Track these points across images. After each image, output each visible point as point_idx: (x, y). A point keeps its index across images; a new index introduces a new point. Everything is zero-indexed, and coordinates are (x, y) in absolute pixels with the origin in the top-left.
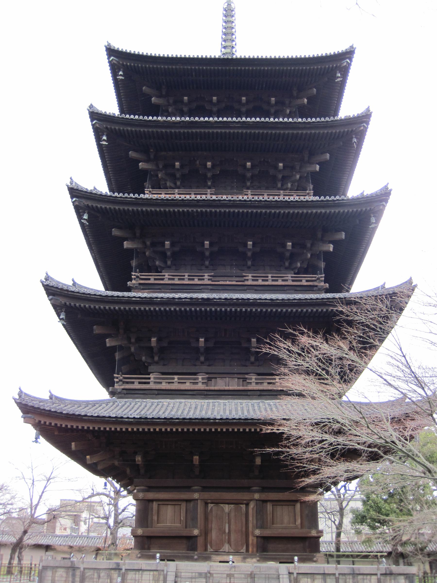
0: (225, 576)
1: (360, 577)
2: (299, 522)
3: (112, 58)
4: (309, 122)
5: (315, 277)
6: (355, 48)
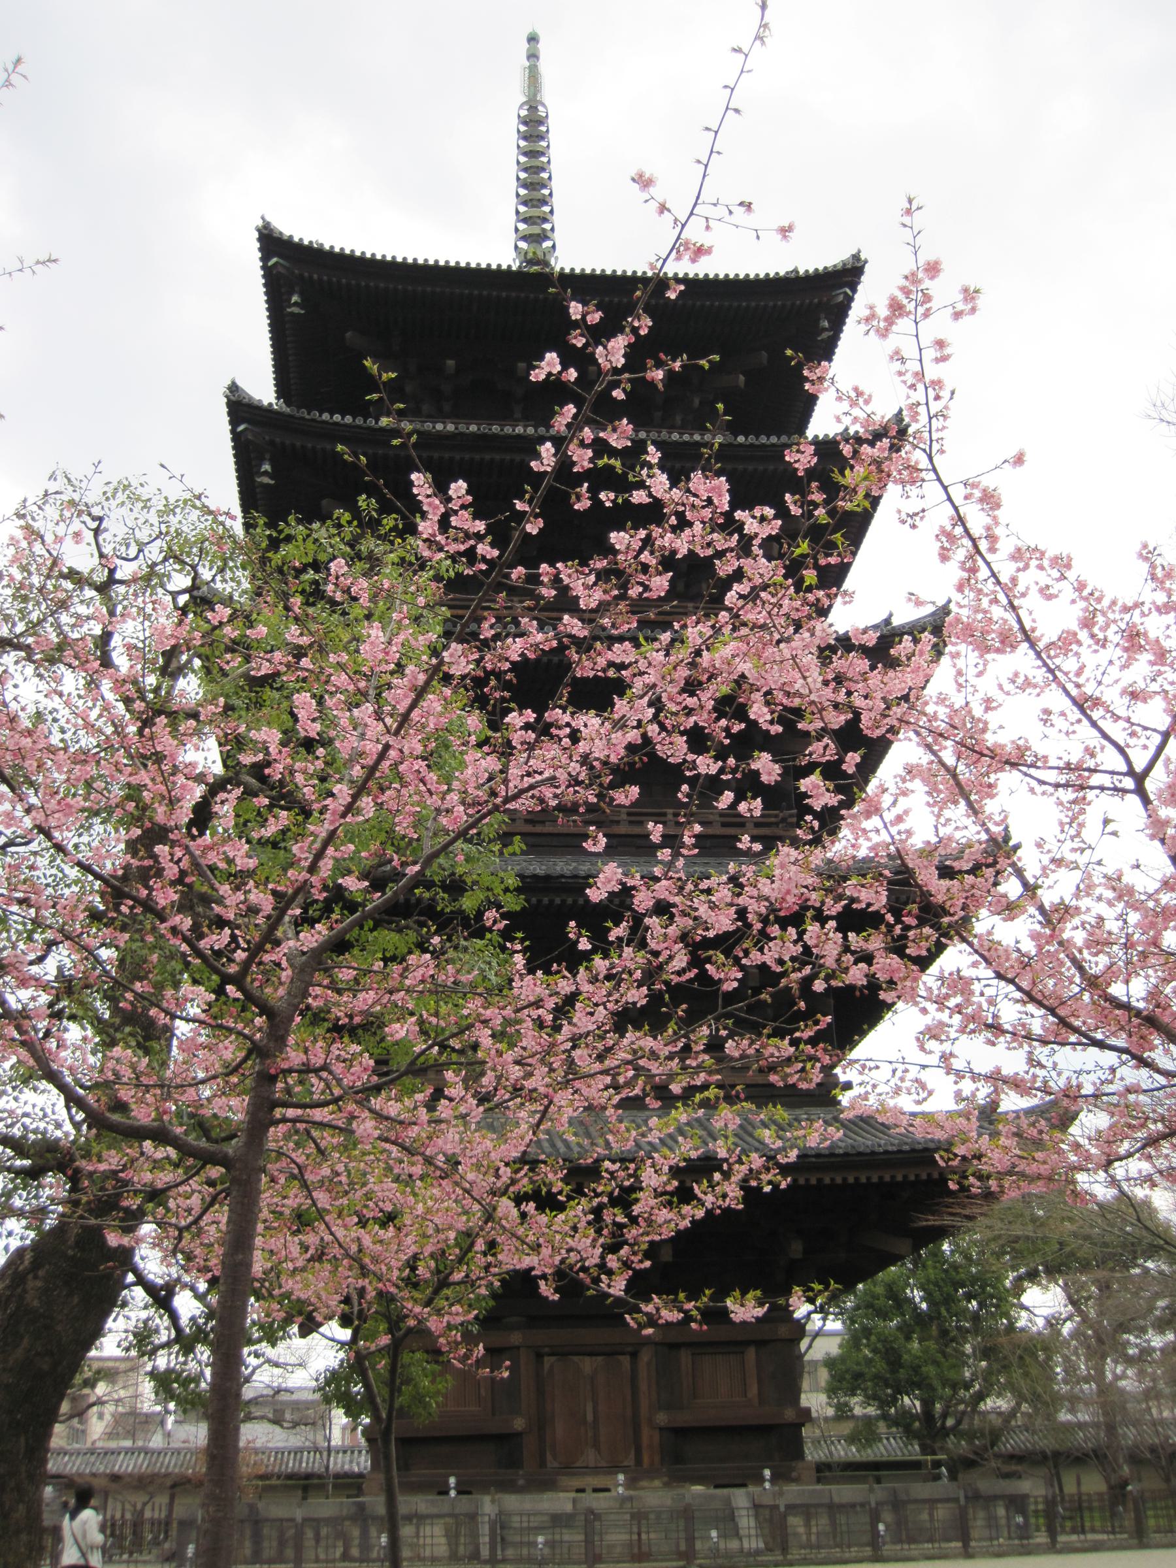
0: (628, 1517)
2: (753, 1390)
3: (275, 260)
5: (776, 816)
6: (866, 262)
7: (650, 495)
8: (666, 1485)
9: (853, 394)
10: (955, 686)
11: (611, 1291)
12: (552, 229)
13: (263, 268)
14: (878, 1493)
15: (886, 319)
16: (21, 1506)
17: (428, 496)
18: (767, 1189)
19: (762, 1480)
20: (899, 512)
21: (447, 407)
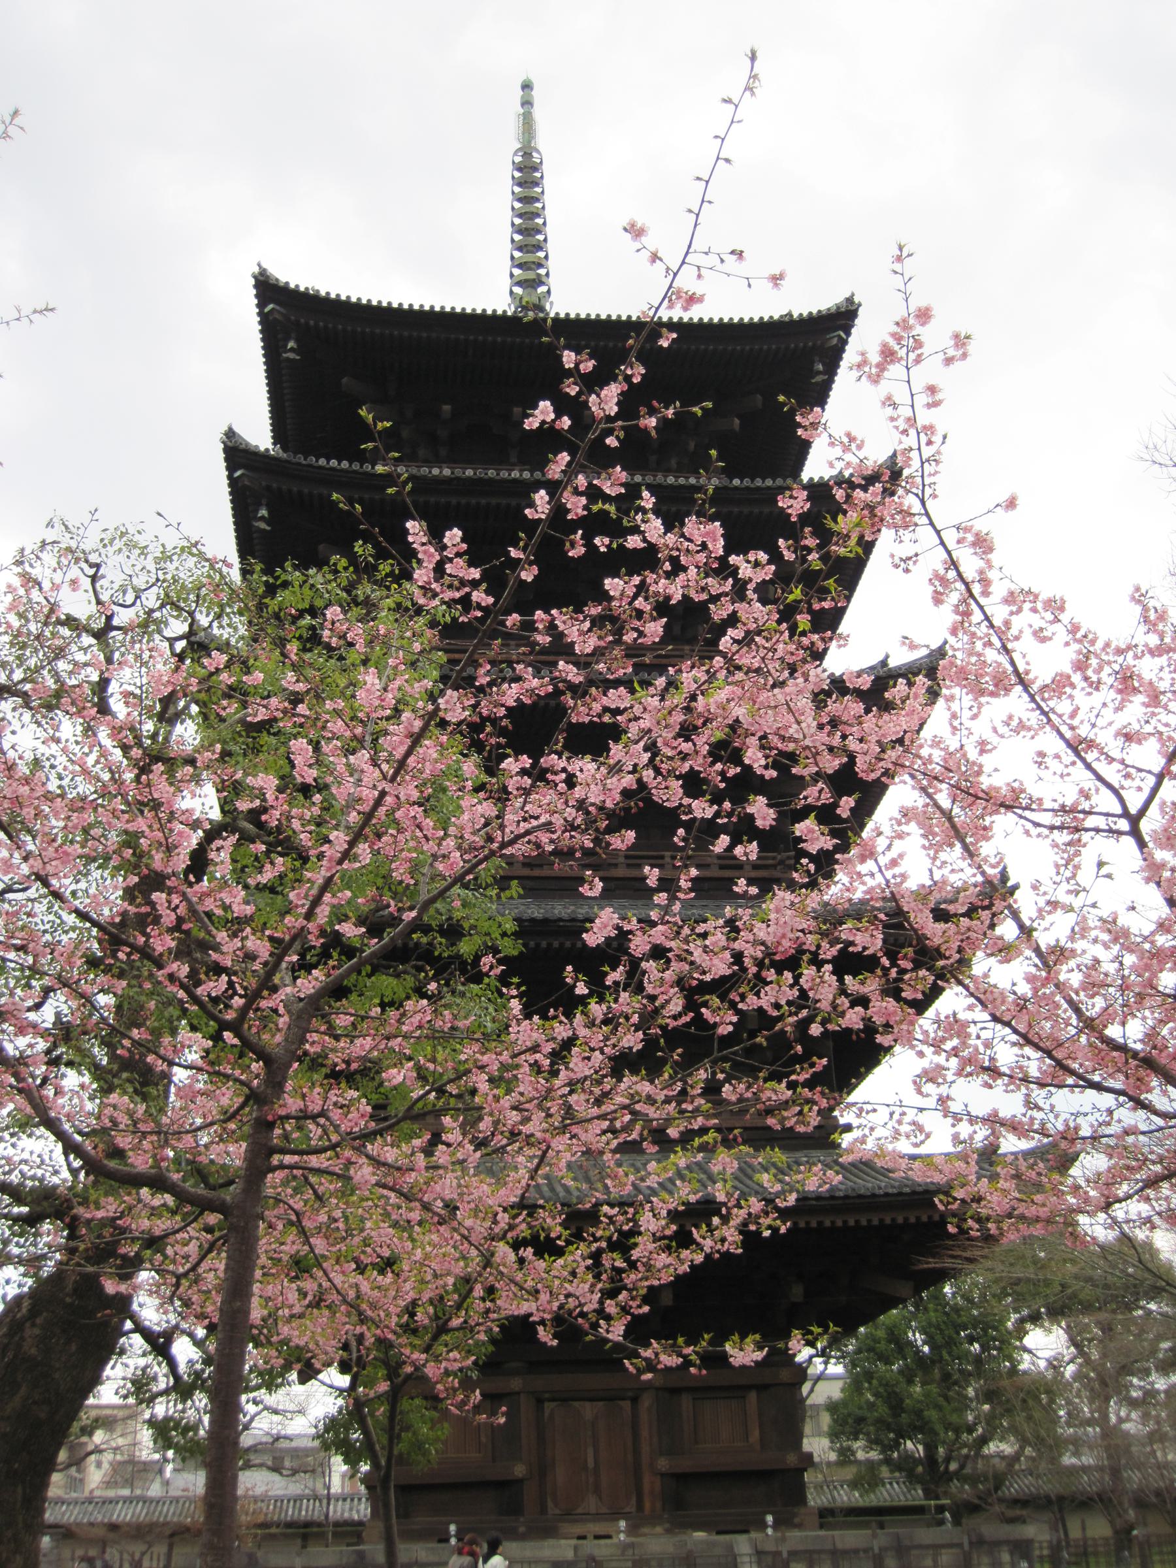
1: (914, 1552)
2: (755, 1435)
3: (271, 306)
4: (758, 489)
5: (774, 858)
6: (860, 305)
7: (645, 540)
8: (668, 1531)
9: (845, 440)
10: (949, 729)
11: (610, 1336)
12: (547, 275)
13: (259, 314)
14: (880, 1539)
15: (877, 366)
16: (18, 1557)
17: (423, 544)
18: (767, 1233)
19: (764, 1526)
20: (892, 556)
21: (443, 452)
